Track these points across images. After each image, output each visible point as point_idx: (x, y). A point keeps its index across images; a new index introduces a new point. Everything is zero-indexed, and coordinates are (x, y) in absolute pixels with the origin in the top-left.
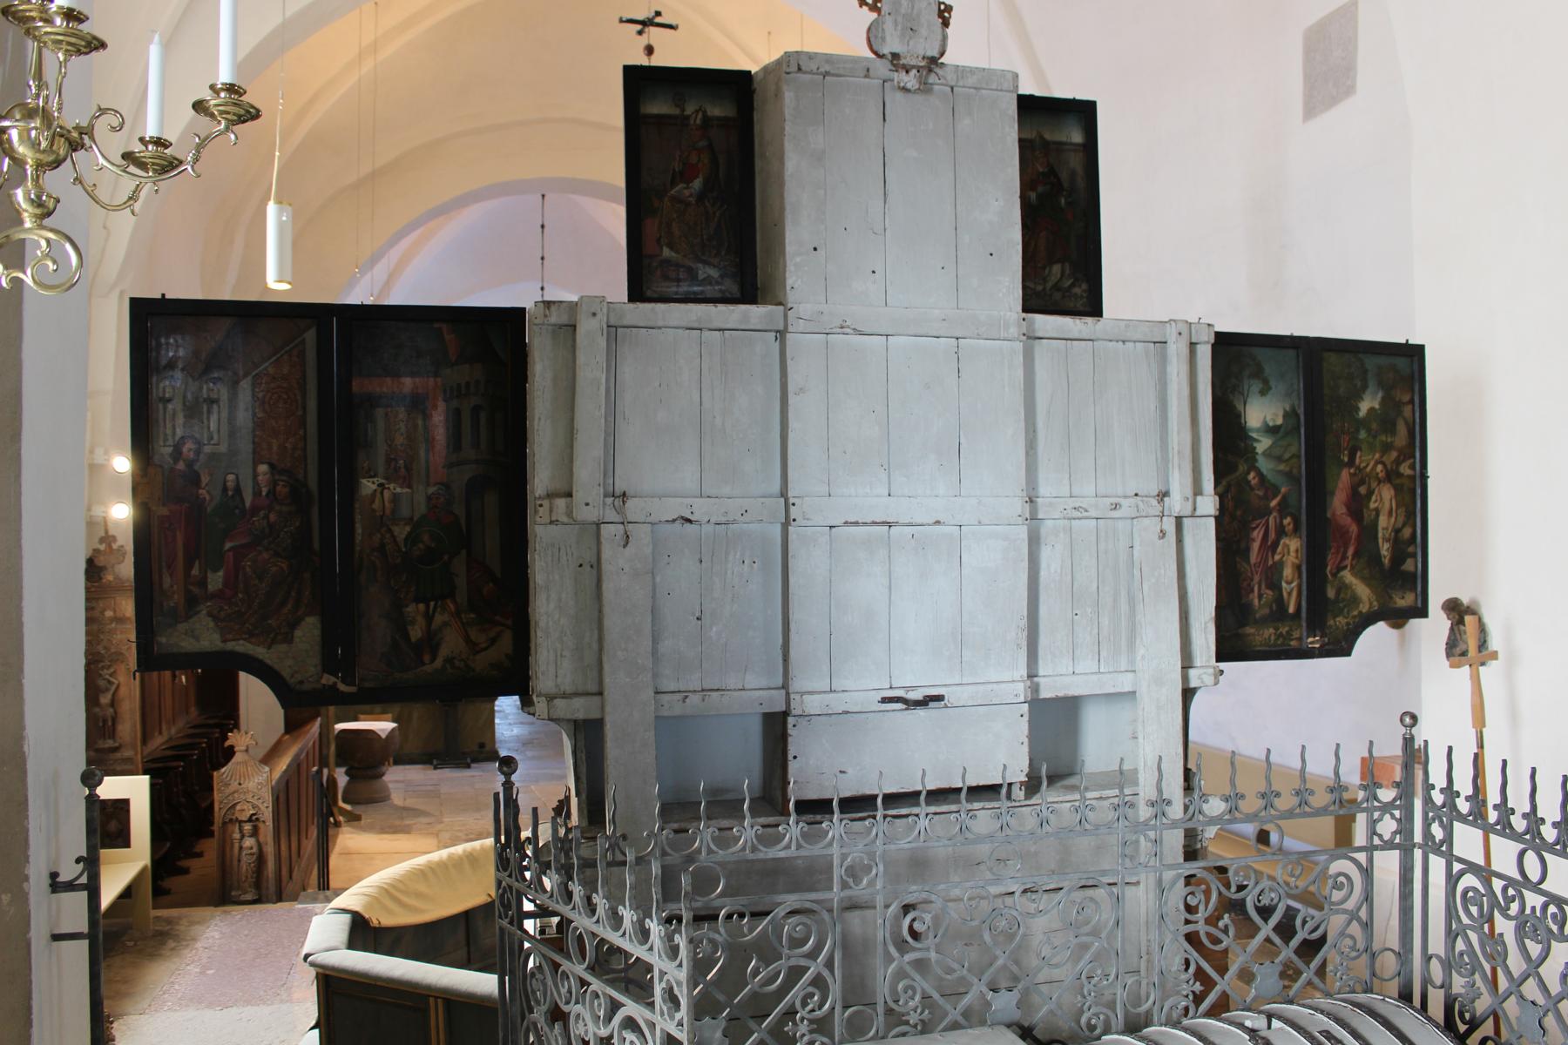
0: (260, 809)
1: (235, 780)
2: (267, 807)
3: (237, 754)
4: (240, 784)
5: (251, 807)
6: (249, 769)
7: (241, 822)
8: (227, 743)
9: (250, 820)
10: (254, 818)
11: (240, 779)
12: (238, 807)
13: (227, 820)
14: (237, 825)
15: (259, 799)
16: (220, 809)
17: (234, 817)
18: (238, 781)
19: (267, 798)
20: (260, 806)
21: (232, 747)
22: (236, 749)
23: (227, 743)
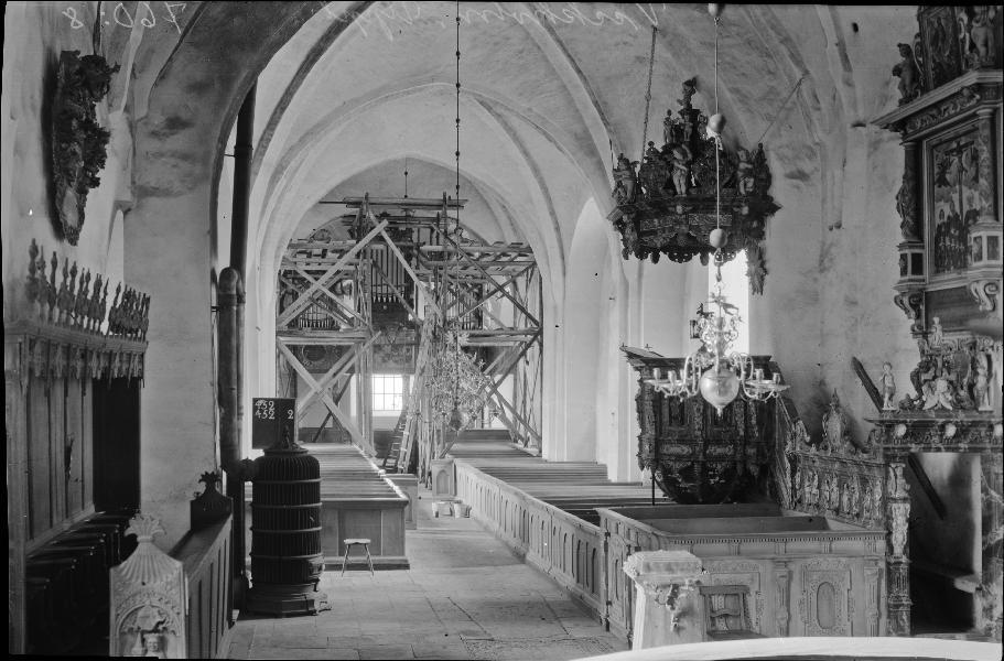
0: (168, 615)
1: (138, 577)
2: (178, 614)
3: (139, 546)
5: (157, 614)
6: (156, 565)
7: (143, 632)
8: (129, 532)
9: (155, 630)
10: (161, 627)
11: (143, 578)
12: (140, 613)
13: (126, 630)
14: (139, 635)
17: (135, 627)
18: (140, 581)
19: (178, 601)
20: (171, 612)
21: (134, 537)
22: (139, 539)
23: (129, 532)
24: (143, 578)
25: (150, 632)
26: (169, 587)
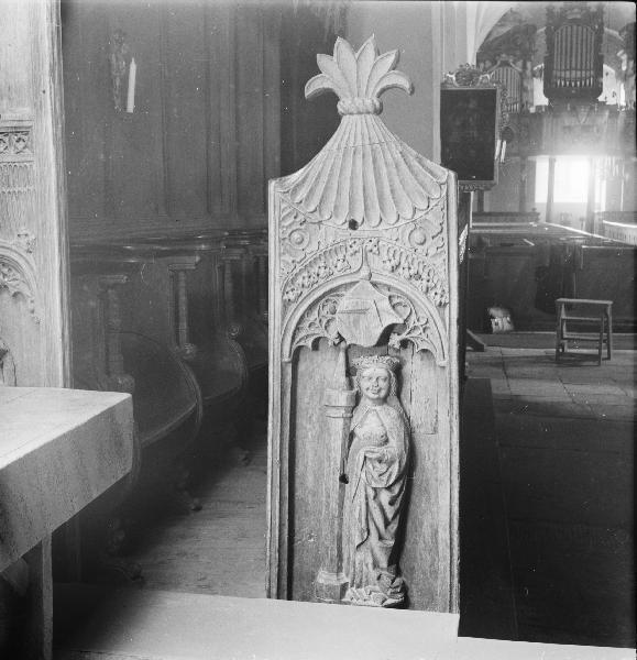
3: (345, 120)
4: (353, 225)
5: (385, 304)
6: (384, 171)
8: (313, 87)
11: (351, 210)
12: (345, 303)
14: (342, 356)
15: (418, 276)
16: (286, 304)
18: (344, 216)
19: (443, 276)
20: (420, 299)
21: (329, 99)
22: (340, 108)
23: (313, 87)
24: (351, 210)
25: (369, 351)
26: (418, 236)
